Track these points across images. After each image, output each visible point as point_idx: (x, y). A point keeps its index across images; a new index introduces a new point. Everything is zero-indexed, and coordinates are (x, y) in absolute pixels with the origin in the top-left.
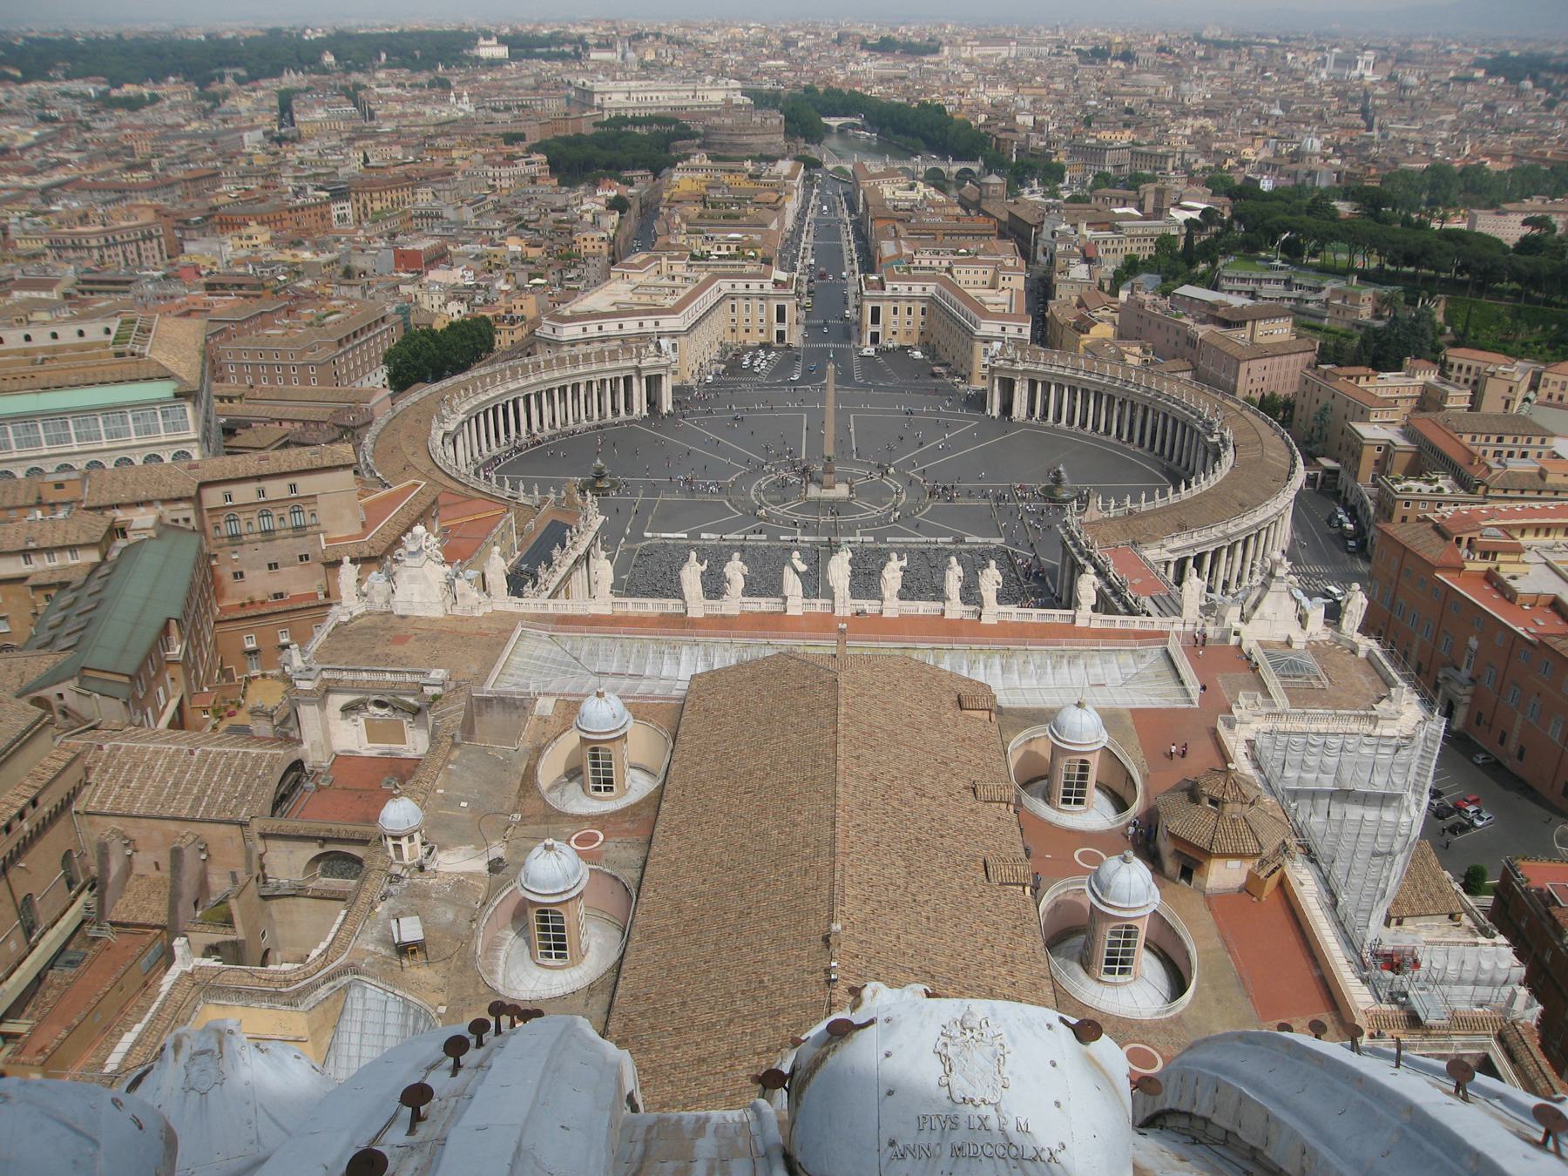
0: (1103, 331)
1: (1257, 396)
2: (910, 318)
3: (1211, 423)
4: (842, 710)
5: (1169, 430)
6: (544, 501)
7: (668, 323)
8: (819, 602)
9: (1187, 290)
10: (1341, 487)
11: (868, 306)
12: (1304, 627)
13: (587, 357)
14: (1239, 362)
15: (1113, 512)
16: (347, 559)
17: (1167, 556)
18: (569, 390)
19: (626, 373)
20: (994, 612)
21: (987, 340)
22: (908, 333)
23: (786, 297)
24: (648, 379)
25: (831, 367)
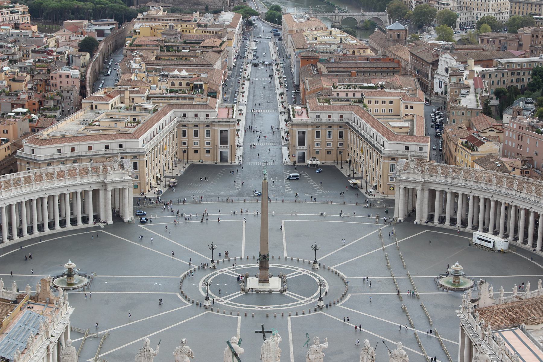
2: (329, 140)
7: (129, 145)
18: (46, 201)
19: (94, 187)
22: (329, 153)
24: (114, 191)
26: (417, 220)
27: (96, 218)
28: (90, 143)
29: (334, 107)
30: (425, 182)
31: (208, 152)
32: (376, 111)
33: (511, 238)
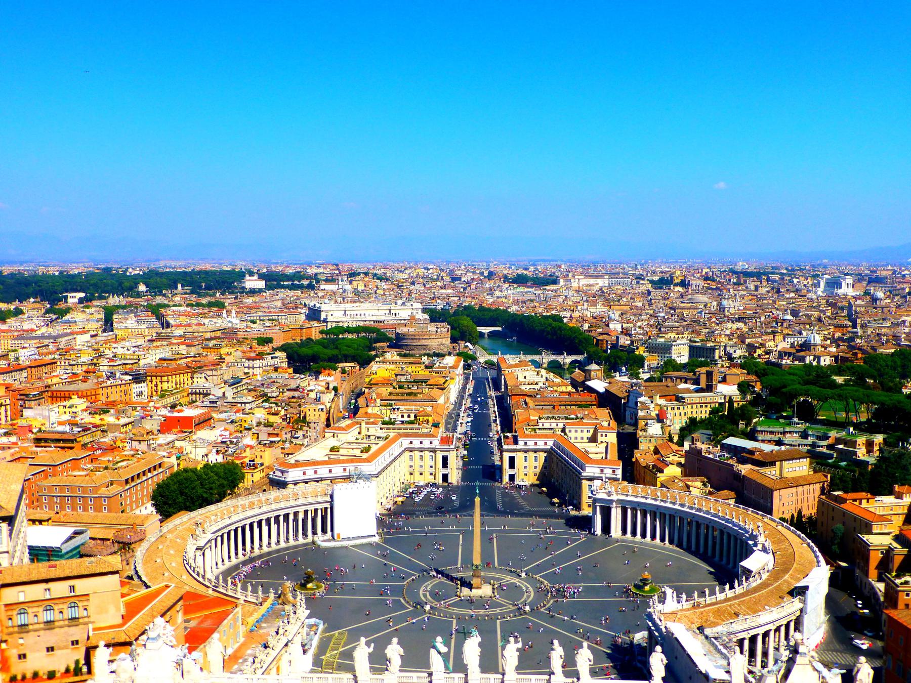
1: (787, 516)
5: (725, 541)
6: (265, 600)
9: (731, 441)
11: (506, 456)
14: (772, 491)
16: (102, 644)
21: (591, 479)
25: (477, 500)
29: (539, 436)
30: (618, 500)
31: (431, 474)
32: (576, 438)
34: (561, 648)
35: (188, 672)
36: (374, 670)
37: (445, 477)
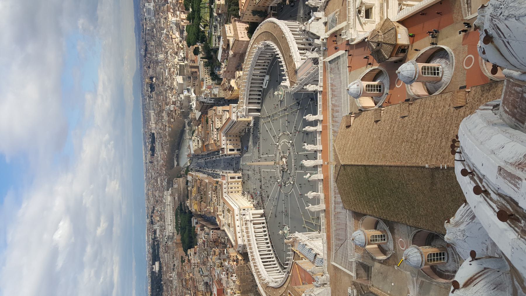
0: (233, 83)
3: (259, 48)
4: (353, 163)
6: (293, 251)
8: (319, 169)
9: (219, 58)
10: (276, 5)
11: (229, 152)
12: (321, 18)
13: (248, 237)
15: (287, 77)
17: (299, 60)
19: (252, 224)
20: (319, 117)
23: (227, 176)
26: (260, 108)
27: (263, 223)
28: (236, 226)
29: (221, 139)
33: (264, 74)
34: (306, 127)
35: (324, 281)
36: (318, 203)
37: (239, 178)
